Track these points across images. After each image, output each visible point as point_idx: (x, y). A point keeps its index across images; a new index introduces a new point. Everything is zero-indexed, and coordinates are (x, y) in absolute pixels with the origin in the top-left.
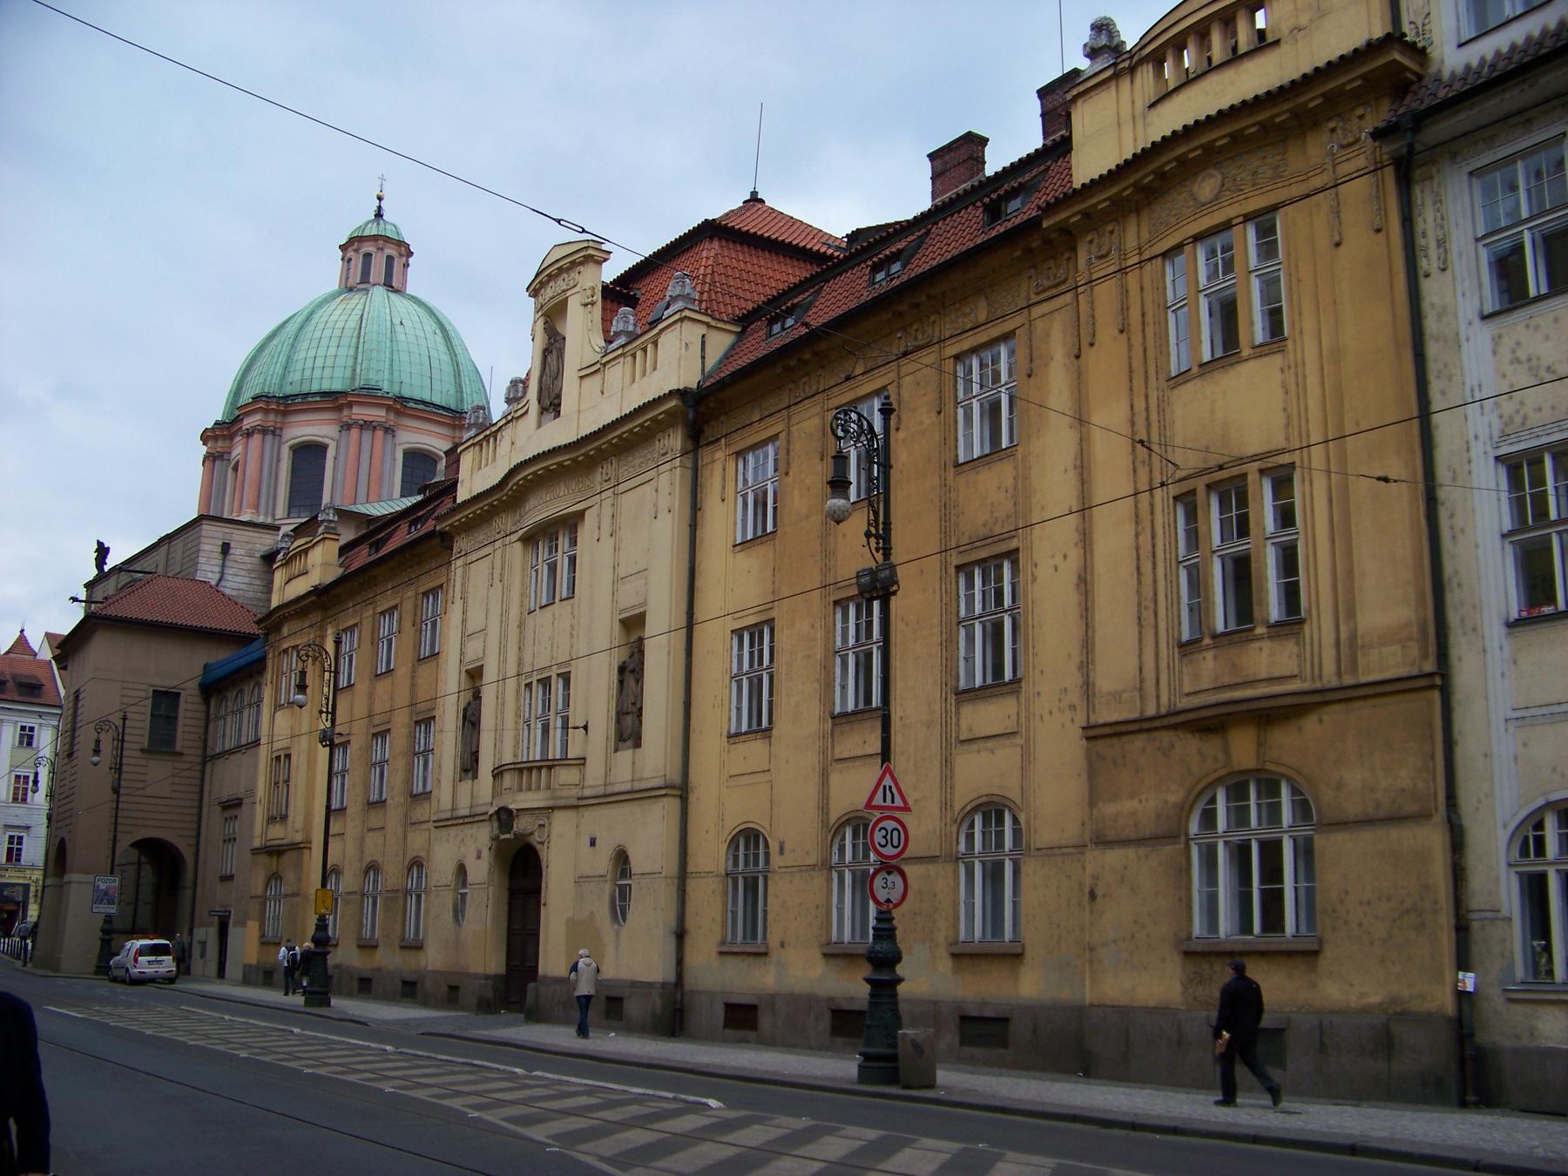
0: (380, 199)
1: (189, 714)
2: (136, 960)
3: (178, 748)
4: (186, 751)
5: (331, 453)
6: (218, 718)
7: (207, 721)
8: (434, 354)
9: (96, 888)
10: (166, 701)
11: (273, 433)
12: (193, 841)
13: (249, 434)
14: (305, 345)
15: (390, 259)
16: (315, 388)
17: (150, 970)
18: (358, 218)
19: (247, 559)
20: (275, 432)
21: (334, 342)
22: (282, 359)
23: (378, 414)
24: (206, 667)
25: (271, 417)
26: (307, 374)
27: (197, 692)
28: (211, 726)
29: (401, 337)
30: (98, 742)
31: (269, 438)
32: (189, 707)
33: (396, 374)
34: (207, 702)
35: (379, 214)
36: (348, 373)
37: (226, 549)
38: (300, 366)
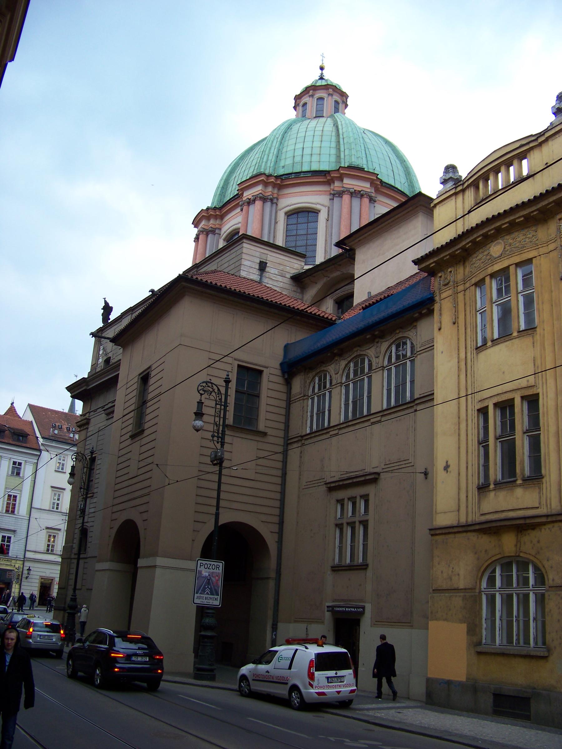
0: (322, 68)
1: (271, 394)
2: (311, 676)
3: (261, 427)
4: (269, 431)
5: (322, 216)
6: (305, 397)
7: (289, 402)
8: (390, 156)
9: (198, 574)
10: (250, 375)
11: (271, 200)
12: (276, 528)
13: (250, 202)
14: (292, 141)
15: (337, 102)
16: (306, 168)
17: (331, 691)
18: (310, 78)
19: (280, 279)
20: (273, 201)
21: (317, 138)
22: (274, 151)
23: (365, 186)
24: (286, 347)
25: (270, 189)
26: (298, 159)
27: (279, 372)
28: (296, 408)
29: (367, 140)
30: (200, 403)
31: (268, 204)
32: (271, 386)
33: (370, 163)
34: (288, 383)
35: (321, 78)
36: (333, 159)
37: (263, 266)
38: (290, 154)
